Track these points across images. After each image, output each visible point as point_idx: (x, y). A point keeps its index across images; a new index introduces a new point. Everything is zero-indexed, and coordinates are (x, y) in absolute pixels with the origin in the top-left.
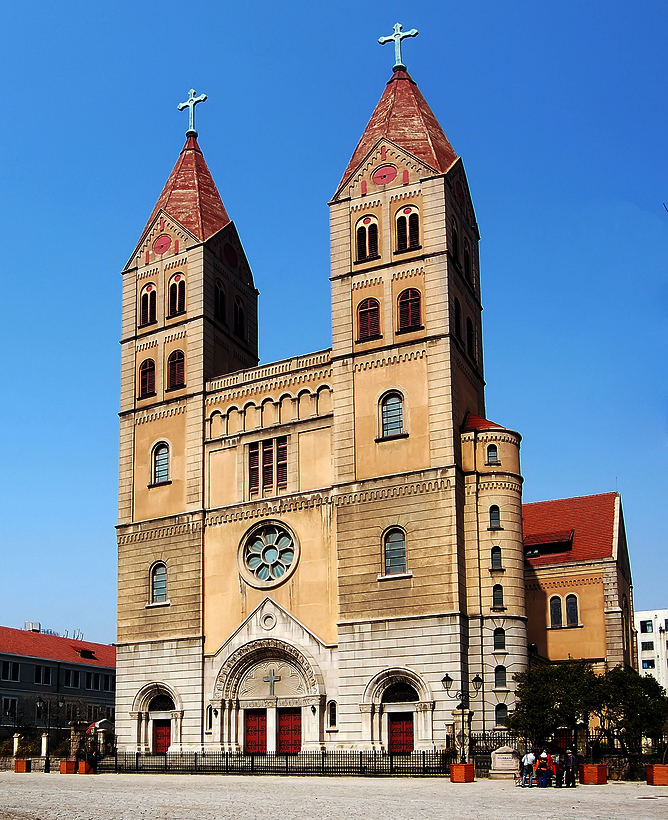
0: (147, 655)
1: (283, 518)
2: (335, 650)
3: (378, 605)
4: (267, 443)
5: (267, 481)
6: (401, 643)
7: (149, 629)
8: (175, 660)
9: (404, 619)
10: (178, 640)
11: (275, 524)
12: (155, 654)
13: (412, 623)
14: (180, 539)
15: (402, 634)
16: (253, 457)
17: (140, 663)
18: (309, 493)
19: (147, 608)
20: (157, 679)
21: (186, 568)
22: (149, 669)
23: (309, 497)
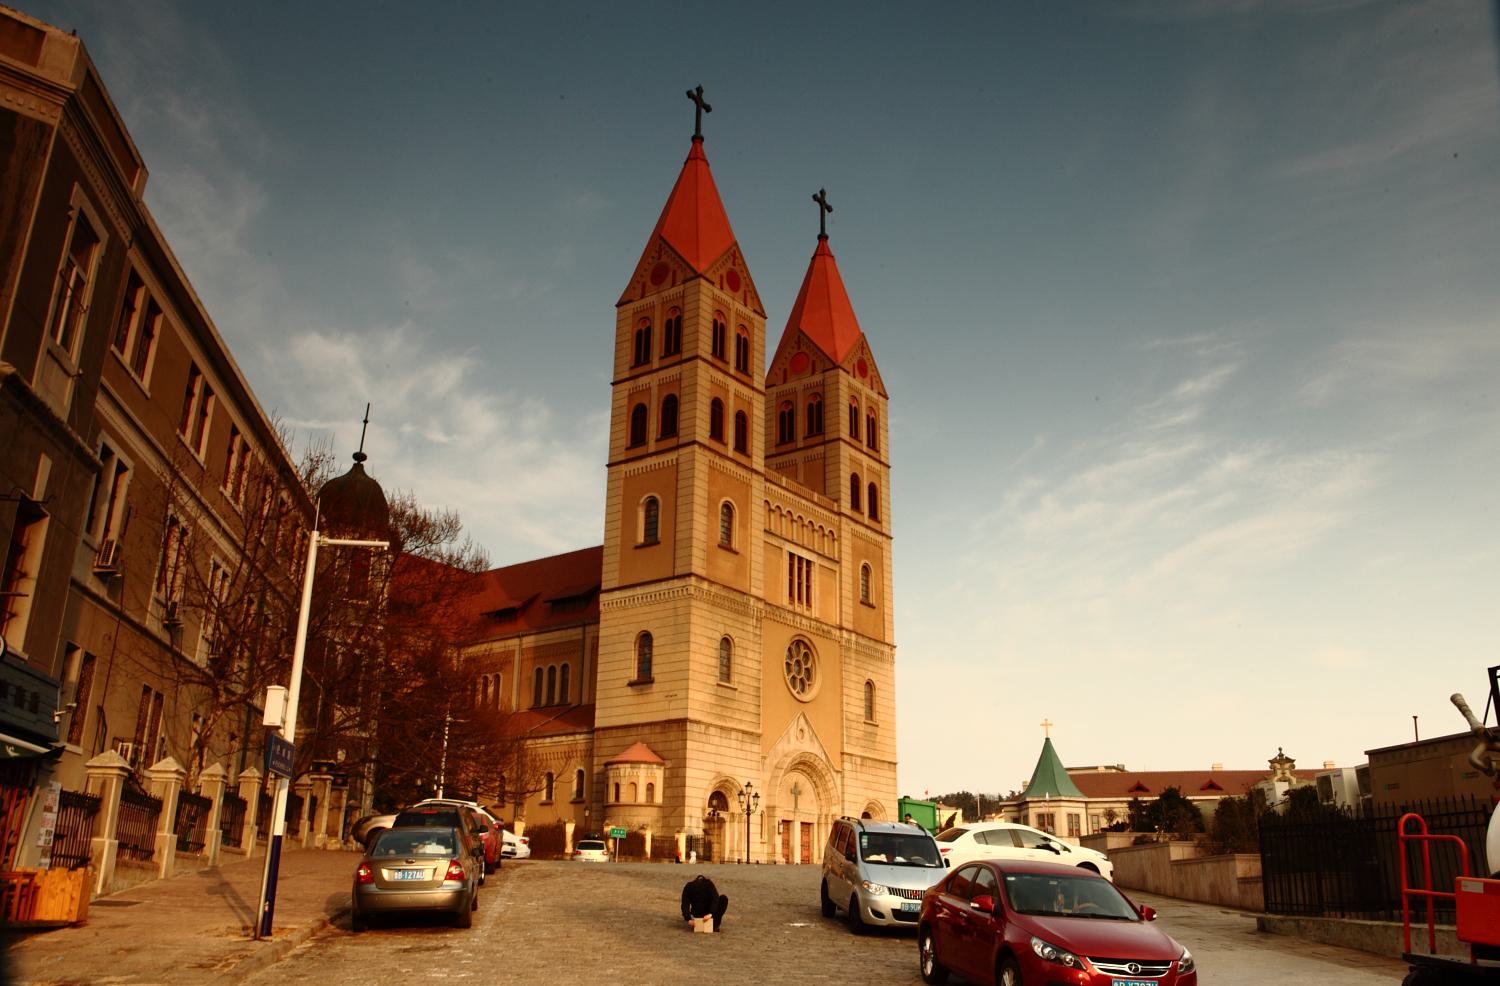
0: (716, 740)
1: (814, 639)
2: (839, 775)
3: (863, 743)
4: (800, 559)
5: (800, 598)
6: (875, 779)
7: (718, 710)
8: (741, 754)
9: (876, 760)
10: (744, 732)
11: (806, 641)
12: (725, 742)
13: (878, 765)
14: (745, 619)
15: (874, 772)
16: (791, 566)
17: (708, 748)
18: (826, 624)
19: (718, 685)
20: (727, 771)
21: (750, 655)
22: (719, 759)
23: (826, 628)
